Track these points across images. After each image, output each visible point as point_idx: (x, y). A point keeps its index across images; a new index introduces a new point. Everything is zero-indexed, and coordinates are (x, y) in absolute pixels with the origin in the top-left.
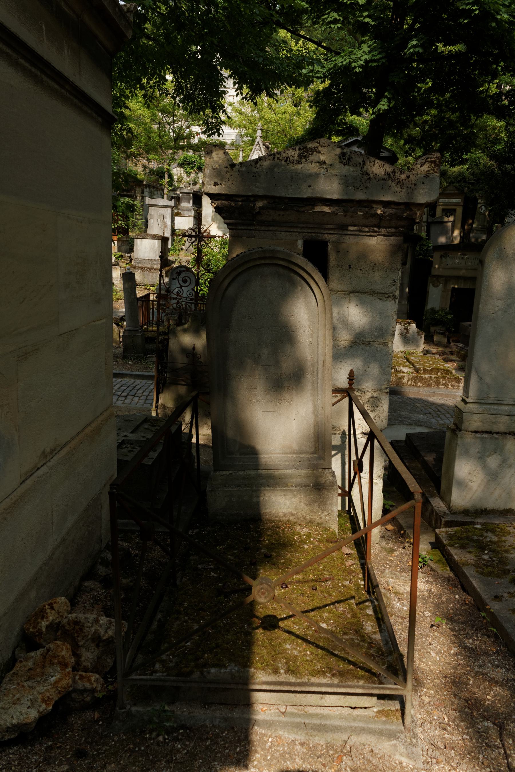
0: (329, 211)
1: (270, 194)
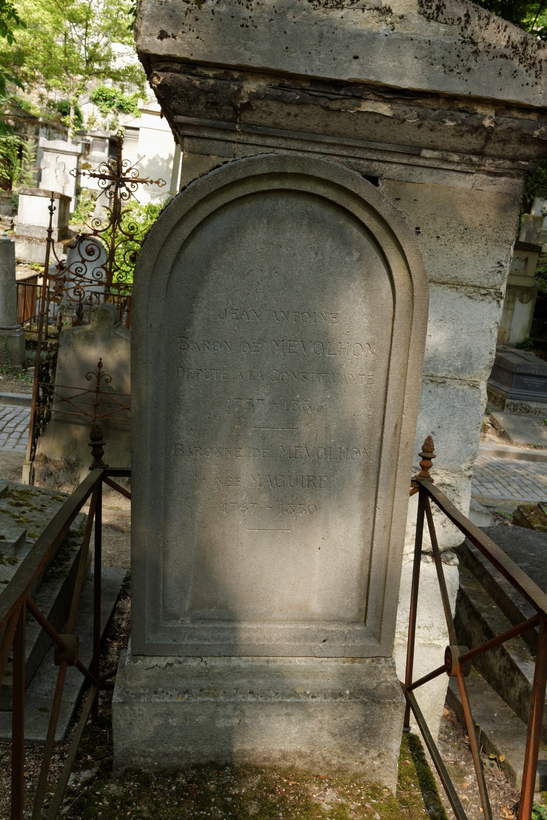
0: (388, 113)
1: (273, 67)
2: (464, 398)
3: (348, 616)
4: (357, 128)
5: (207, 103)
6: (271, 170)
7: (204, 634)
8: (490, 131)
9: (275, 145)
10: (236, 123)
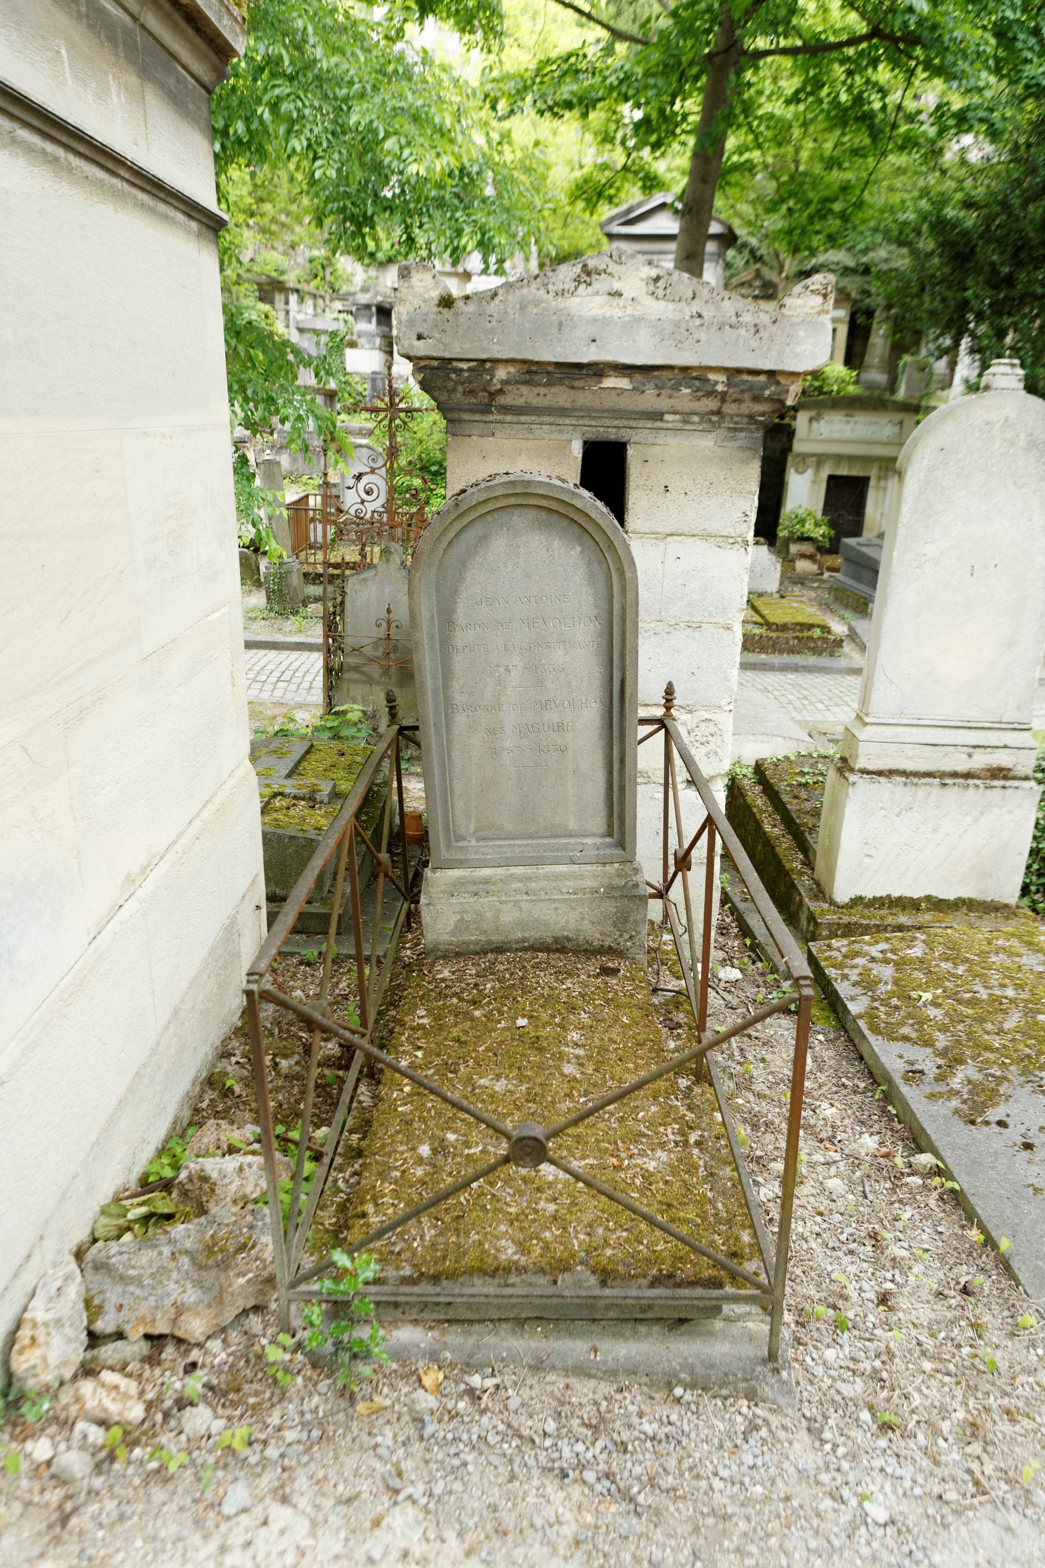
0: (629, 387)
8: (724, 394)
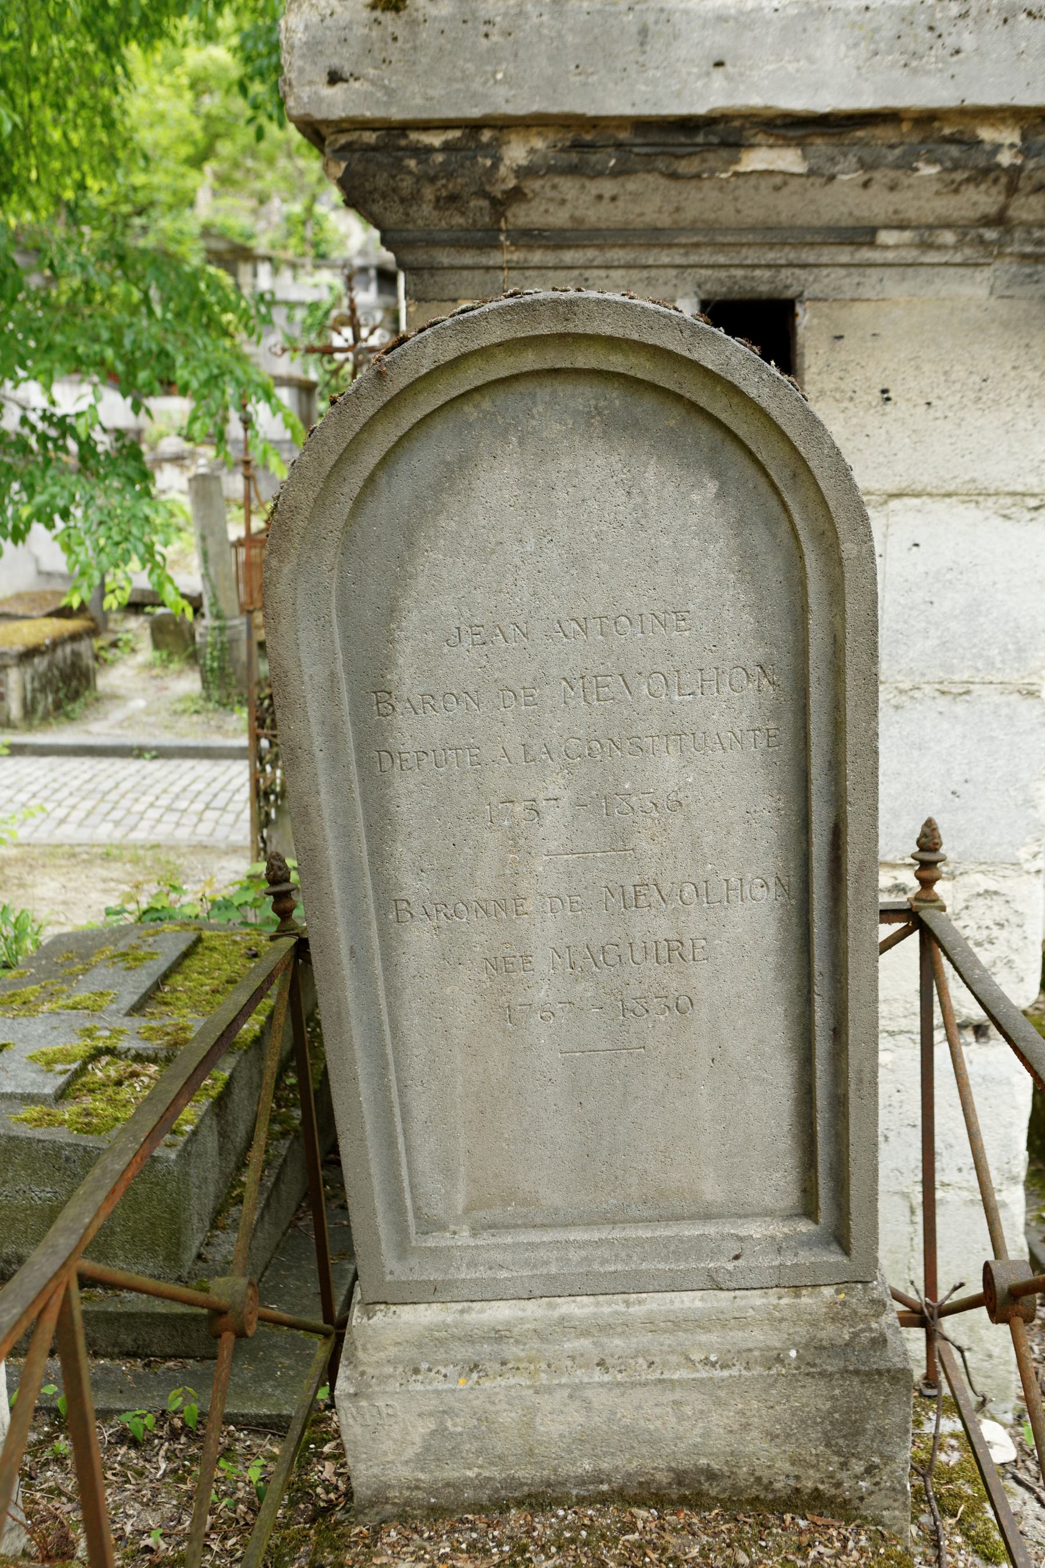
0: (800, 168)
1: (554, 109)
2: (1011, 719)
3: (782, 1205)
4: (739, 206)
5: (438, 199)
6: (509, 336)
7: (498, 1256)
8: (1015, 171)
9: (581, 262)
10: (500, 230)
